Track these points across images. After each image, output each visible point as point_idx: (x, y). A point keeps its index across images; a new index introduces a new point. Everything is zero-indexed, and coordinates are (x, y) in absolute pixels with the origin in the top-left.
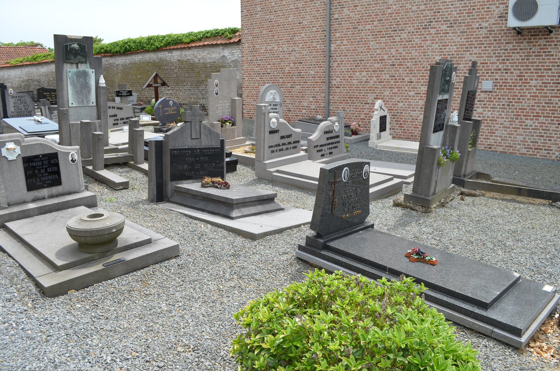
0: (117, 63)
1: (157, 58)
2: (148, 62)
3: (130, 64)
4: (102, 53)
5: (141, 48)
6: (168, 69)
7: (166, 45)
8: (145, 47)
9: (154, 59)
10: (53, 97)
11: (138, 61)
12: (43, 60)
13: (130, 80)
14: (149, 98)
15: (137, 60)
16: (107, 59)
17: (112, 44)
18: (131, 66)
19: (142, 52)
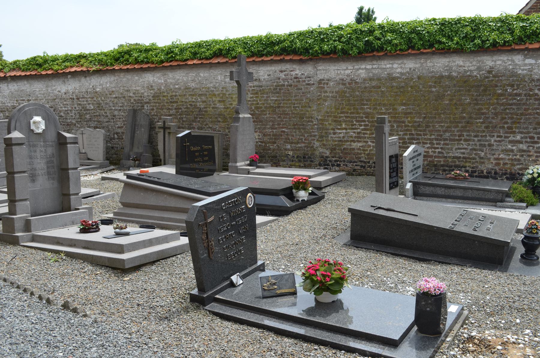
0: (321, 75)
1: (479, 69)
2: (442, 77)
3: (371, 79)
4: (269, 54)
5: (423, 45)
6: (520, 95)
7: (521, 40)
8: (440, 42)
9: (466, 71)
10: (206, 156)
11: (402, 74)
12: (66, 67)
13: (367, 115)
14: (439, 157)
15: (399, 70)
16: (284, 68)
17: (301, 34)
18: (374, 83)
19: (427, 53)
